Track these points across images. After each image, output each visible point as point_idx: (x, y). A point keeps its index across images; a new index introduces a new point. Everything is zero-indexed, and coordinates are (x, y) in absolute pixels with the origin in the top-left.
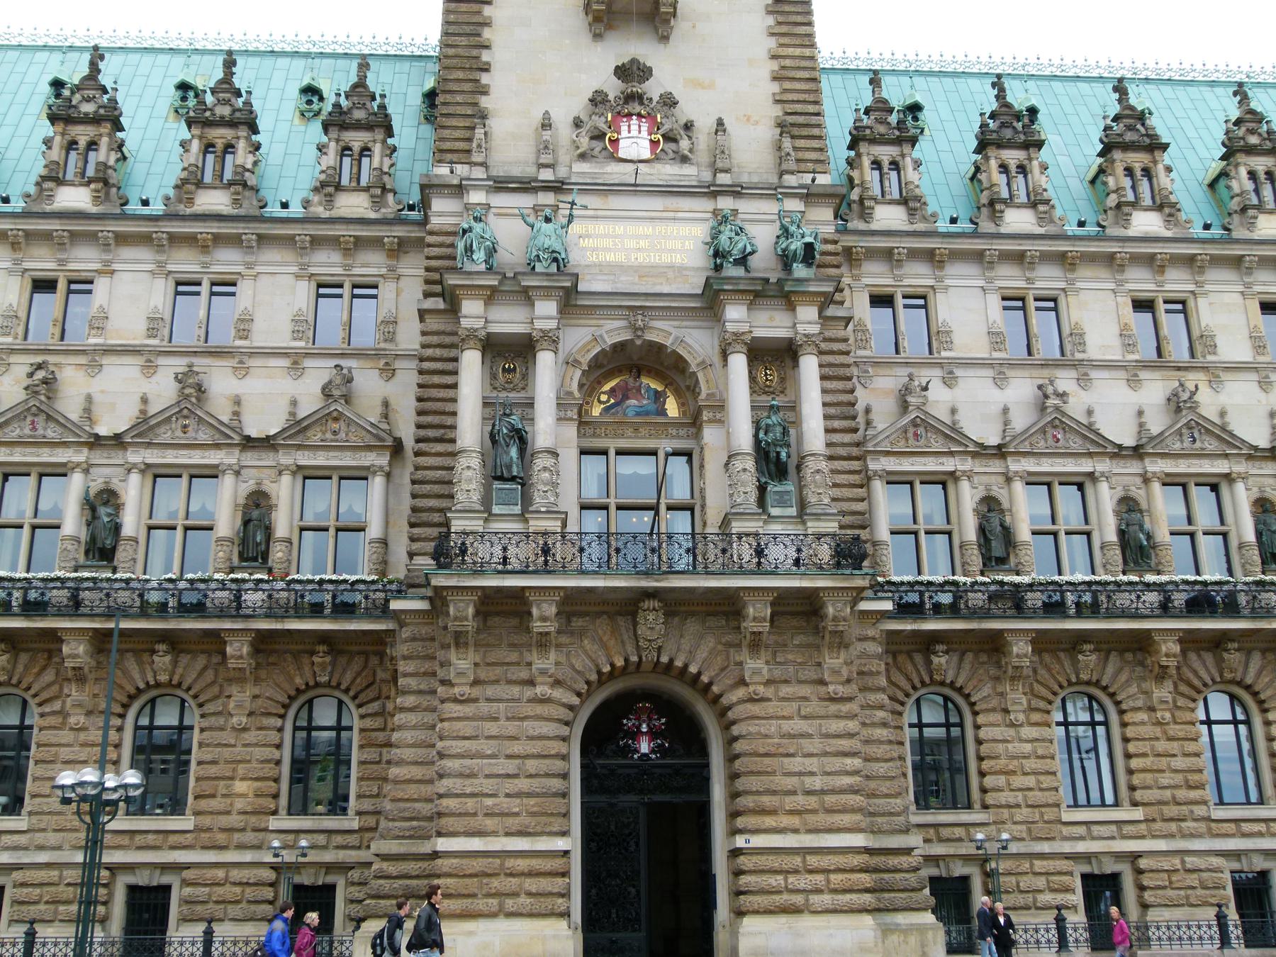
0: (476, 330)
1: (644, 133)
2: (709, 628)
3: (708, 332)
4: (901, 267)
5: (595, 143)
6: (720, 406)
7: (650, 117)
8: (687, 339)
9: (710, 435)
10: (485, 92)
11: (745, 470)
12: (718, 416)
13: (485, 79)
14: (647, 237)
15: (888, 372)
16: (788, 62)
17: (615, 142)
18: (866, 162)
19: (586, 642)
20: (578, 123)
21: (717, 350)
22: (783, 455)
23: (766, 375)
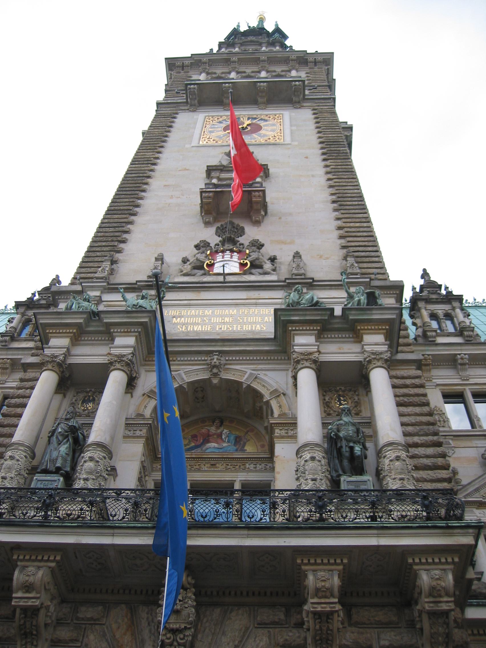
0: (56, 357)
1: (236, 260)
2: (262, 625)
3: (284, 373)
4: (466, 370)
5: (196, 271)
6: (292, 424)
7: (239, 252)
8: (262, 376)
9: (283, 450)
10: (119, 252)
11: (313, 459)
12: (291, 433)
13: (122, 245)
14: (231, 316)
15: (469, 444)
16: (349, 230)
17: (211, 266)
18: (425, 313)
19: (92, 637)
20: (185, 261)
21: (291, 381)
22: (357, 449)
23: (340, 400)
